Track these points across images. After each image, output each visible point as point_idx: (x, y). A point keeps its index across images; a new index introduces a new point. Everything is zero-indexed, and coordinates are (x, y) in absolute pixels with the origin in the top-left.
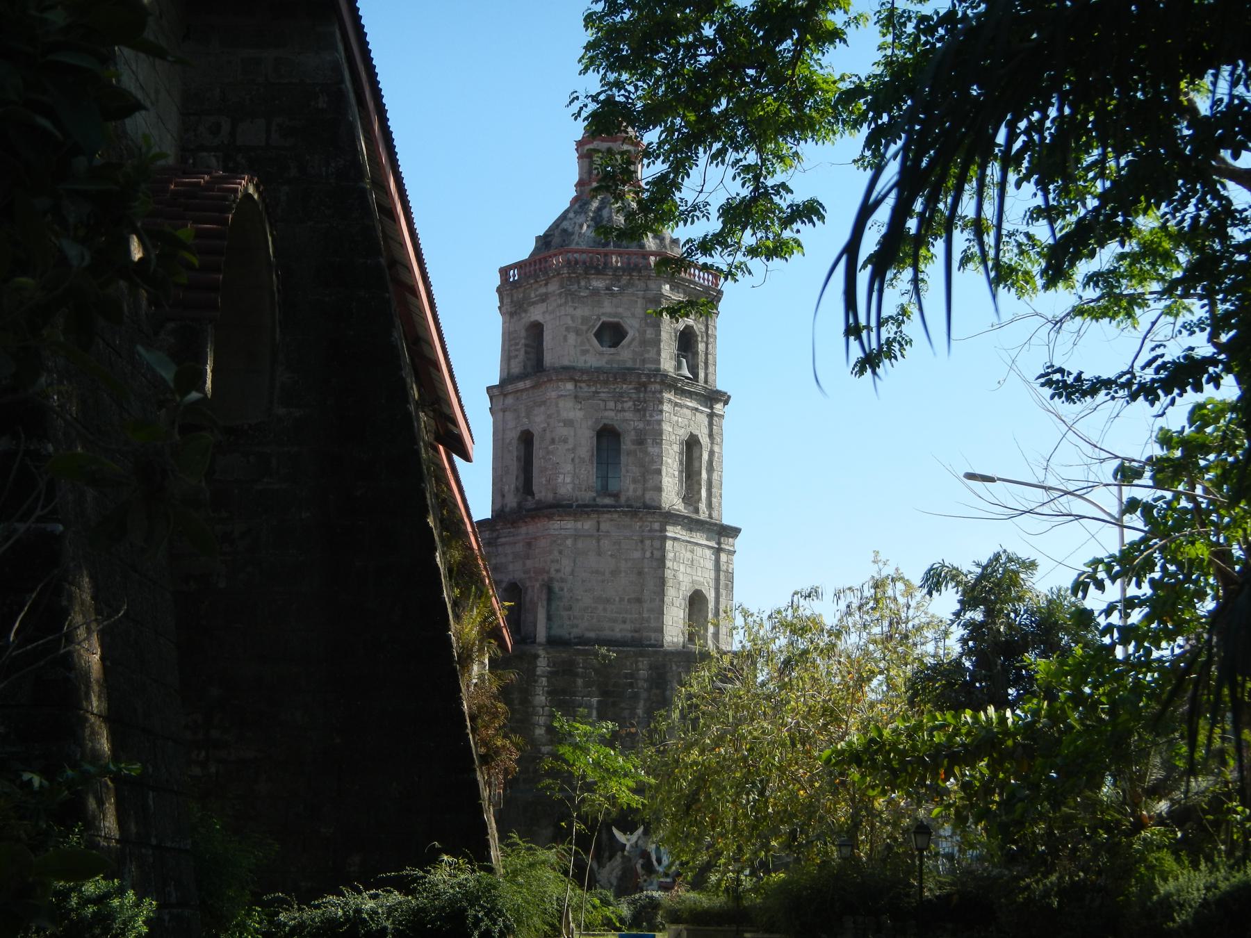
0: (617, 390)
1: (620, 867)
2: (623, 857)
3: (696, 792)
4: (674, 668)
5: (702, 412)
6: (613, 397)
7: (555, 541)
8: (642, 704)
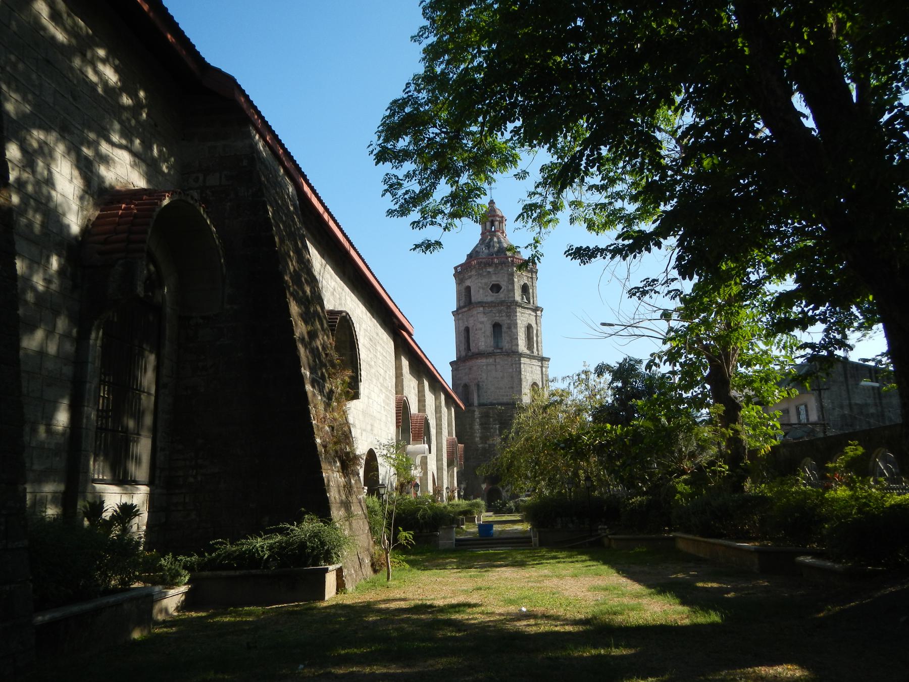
3: (512, 462)
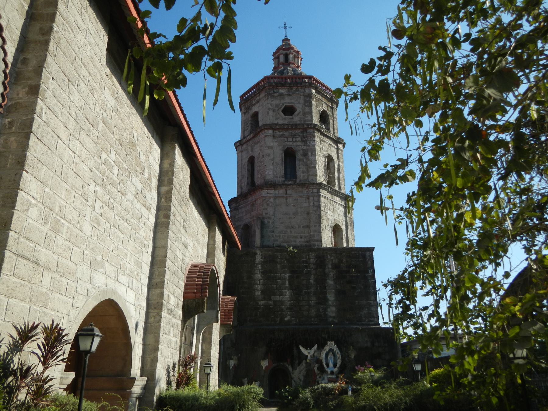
1: (305, 369)
2: (307, 363)
4: (329, 257)
5: (333, 147)
6: (292, 135)
8: (312, 277)
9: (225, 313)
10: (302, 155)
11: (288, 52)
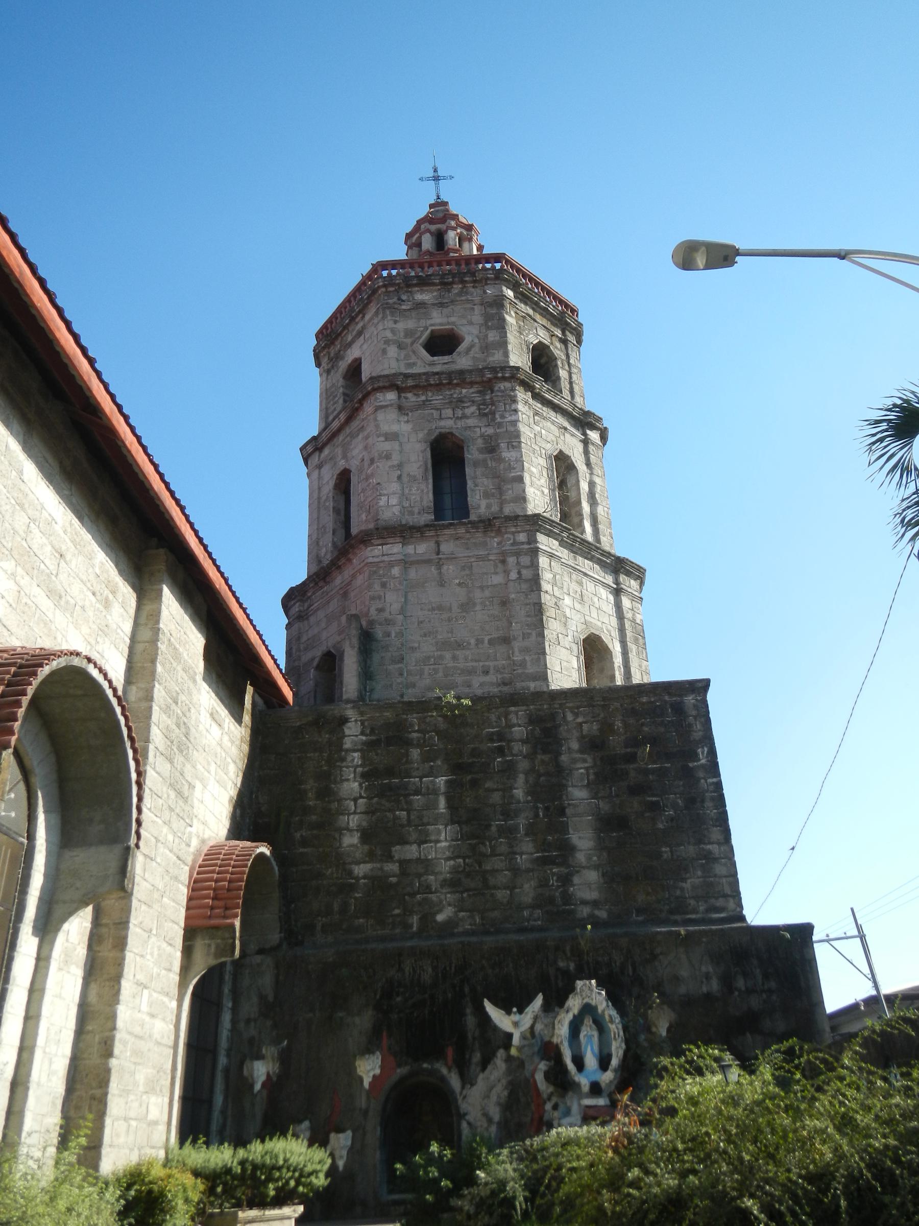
0: (455, 396)
1: (504, 1082)
2: (509, 1059)
4: (570, 717)
7: (375, 572)
8: (521, 778)
9: (215, 890)
10: (481, 451)
11: (442, 227)
